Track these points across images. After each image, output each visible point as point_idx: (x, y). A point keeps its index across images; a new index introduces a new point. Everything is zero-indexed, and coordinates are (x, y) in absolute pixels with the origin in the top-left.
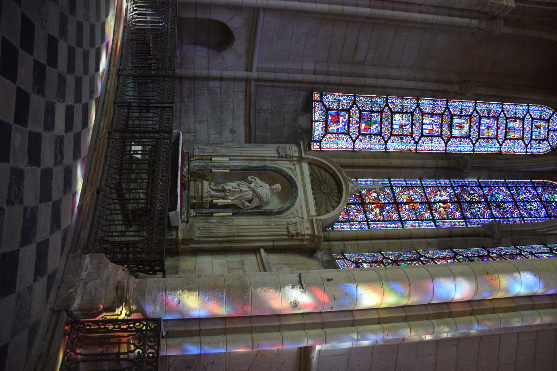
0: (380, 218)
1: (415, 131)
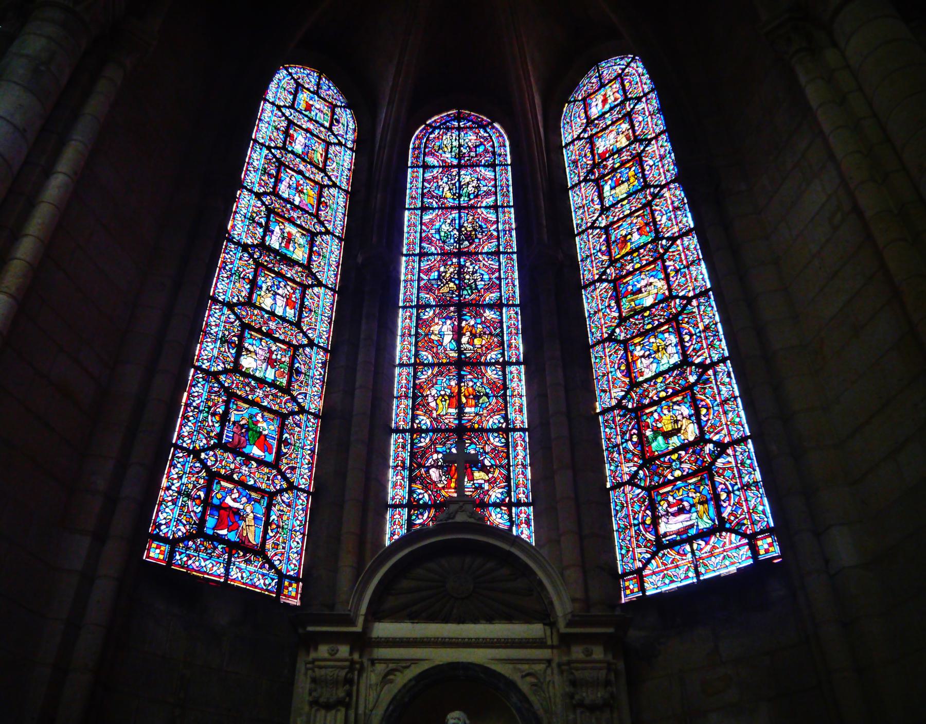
0: (500, 473)
1: (286, 337)
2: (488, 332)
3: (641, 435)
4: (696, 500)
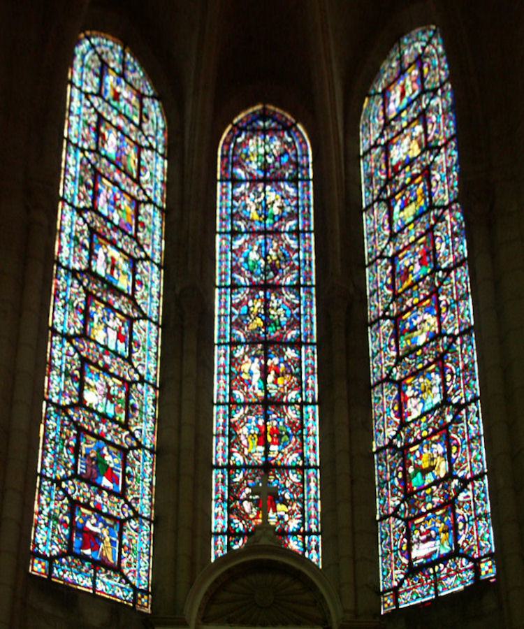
3: (405, 472)
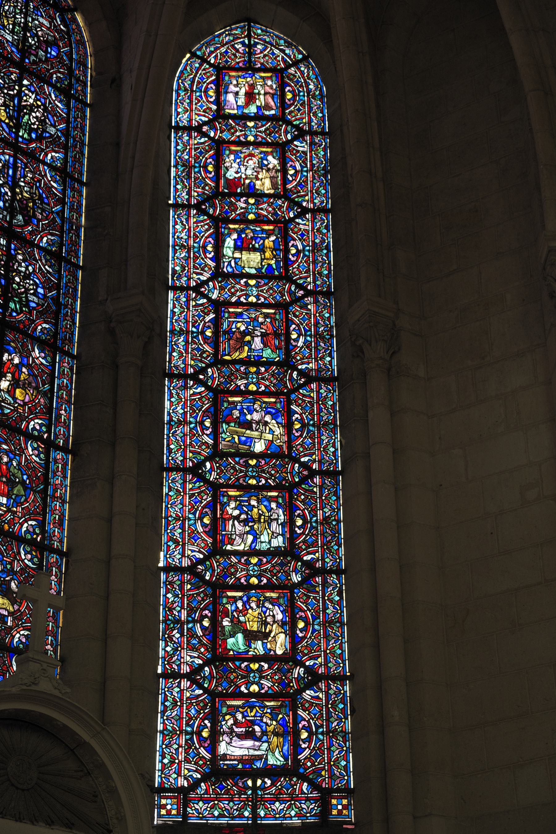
2: (34, 385)
4: (271, 728)
